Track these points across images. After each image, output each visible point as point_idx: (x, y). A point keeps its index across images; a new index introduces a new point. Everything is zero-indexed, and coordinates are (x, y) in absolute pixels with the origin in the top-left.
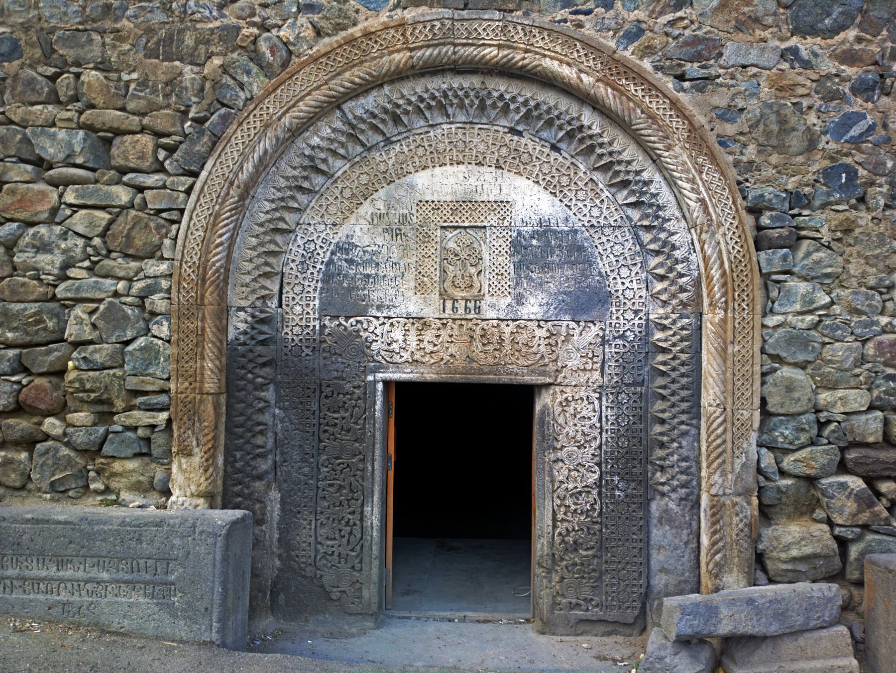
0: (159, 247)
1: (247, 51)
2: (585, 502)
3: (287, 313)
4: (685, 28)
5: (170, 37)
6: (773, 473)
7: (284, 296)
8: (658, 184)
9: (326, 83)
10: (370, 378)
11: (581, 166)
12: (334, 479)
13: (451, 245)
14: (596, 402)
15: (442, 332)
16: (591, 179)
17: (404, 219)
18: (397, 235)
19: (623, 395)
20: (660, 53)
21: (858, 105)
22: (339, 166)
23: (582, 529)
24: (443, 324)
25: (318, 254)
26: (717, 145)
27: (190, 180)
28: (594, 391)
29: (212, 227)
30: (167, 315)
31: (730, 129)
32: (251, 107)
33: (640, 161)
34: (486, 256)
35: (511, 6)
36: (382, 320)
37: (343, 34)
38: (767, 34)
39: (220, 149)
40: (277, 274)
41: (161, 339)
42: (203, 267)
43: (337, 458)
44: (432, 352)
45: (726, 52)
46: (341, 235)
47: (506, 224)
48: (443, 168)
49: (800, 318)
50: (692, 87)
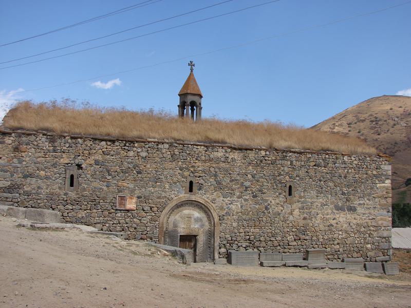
21: (229, 206)
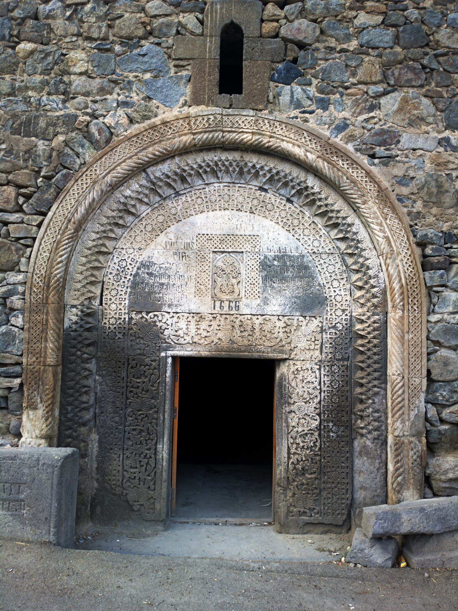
0: (18, 263)
1: (82, 132)
2: (309, 441)
3: (106, 309)
4: (375, 124)
5: (29, 121)
6: (436, 421)
7: (104, 297)
8: (358, 227)
9: (136, 155)
10: (163, 354)
11: (306, 213)
12: (137, 425)
13: (220, 264)
14: (317, 372)
15: (212, 323)
16: (313, 222)
17: (188, 246)
18: (183, 257)
19: (335, 367)
20: (359, 140)
22: (143, 210)
23: (308, 460)
24: (214, 317)
25: (128, 269)
26: (396, 201)
27: (41, 218)
28: (316, 364)
29: (55, 249)
30: (22, 311)
31: (405, 191)
32: (84, 169)
33: (346, 210)
34: (243, 272)
35: (260, 107)
36: (172, 314)
37: (148, 122)
38: (429, 128)
39: (62, 197)
40: (99, 282)
41: (17, 327)
42: (48, 278)
43: (139, 411)
44: (206, 337)
45: (403, 140)
46: (144, 256)
47: (257, 250)
48: (214, 212)
49: (452, 316)
50: (380, 163)
